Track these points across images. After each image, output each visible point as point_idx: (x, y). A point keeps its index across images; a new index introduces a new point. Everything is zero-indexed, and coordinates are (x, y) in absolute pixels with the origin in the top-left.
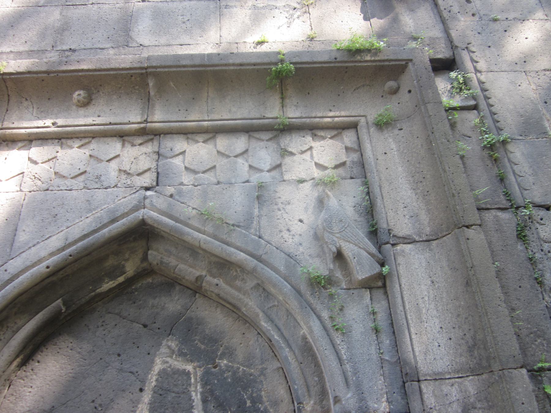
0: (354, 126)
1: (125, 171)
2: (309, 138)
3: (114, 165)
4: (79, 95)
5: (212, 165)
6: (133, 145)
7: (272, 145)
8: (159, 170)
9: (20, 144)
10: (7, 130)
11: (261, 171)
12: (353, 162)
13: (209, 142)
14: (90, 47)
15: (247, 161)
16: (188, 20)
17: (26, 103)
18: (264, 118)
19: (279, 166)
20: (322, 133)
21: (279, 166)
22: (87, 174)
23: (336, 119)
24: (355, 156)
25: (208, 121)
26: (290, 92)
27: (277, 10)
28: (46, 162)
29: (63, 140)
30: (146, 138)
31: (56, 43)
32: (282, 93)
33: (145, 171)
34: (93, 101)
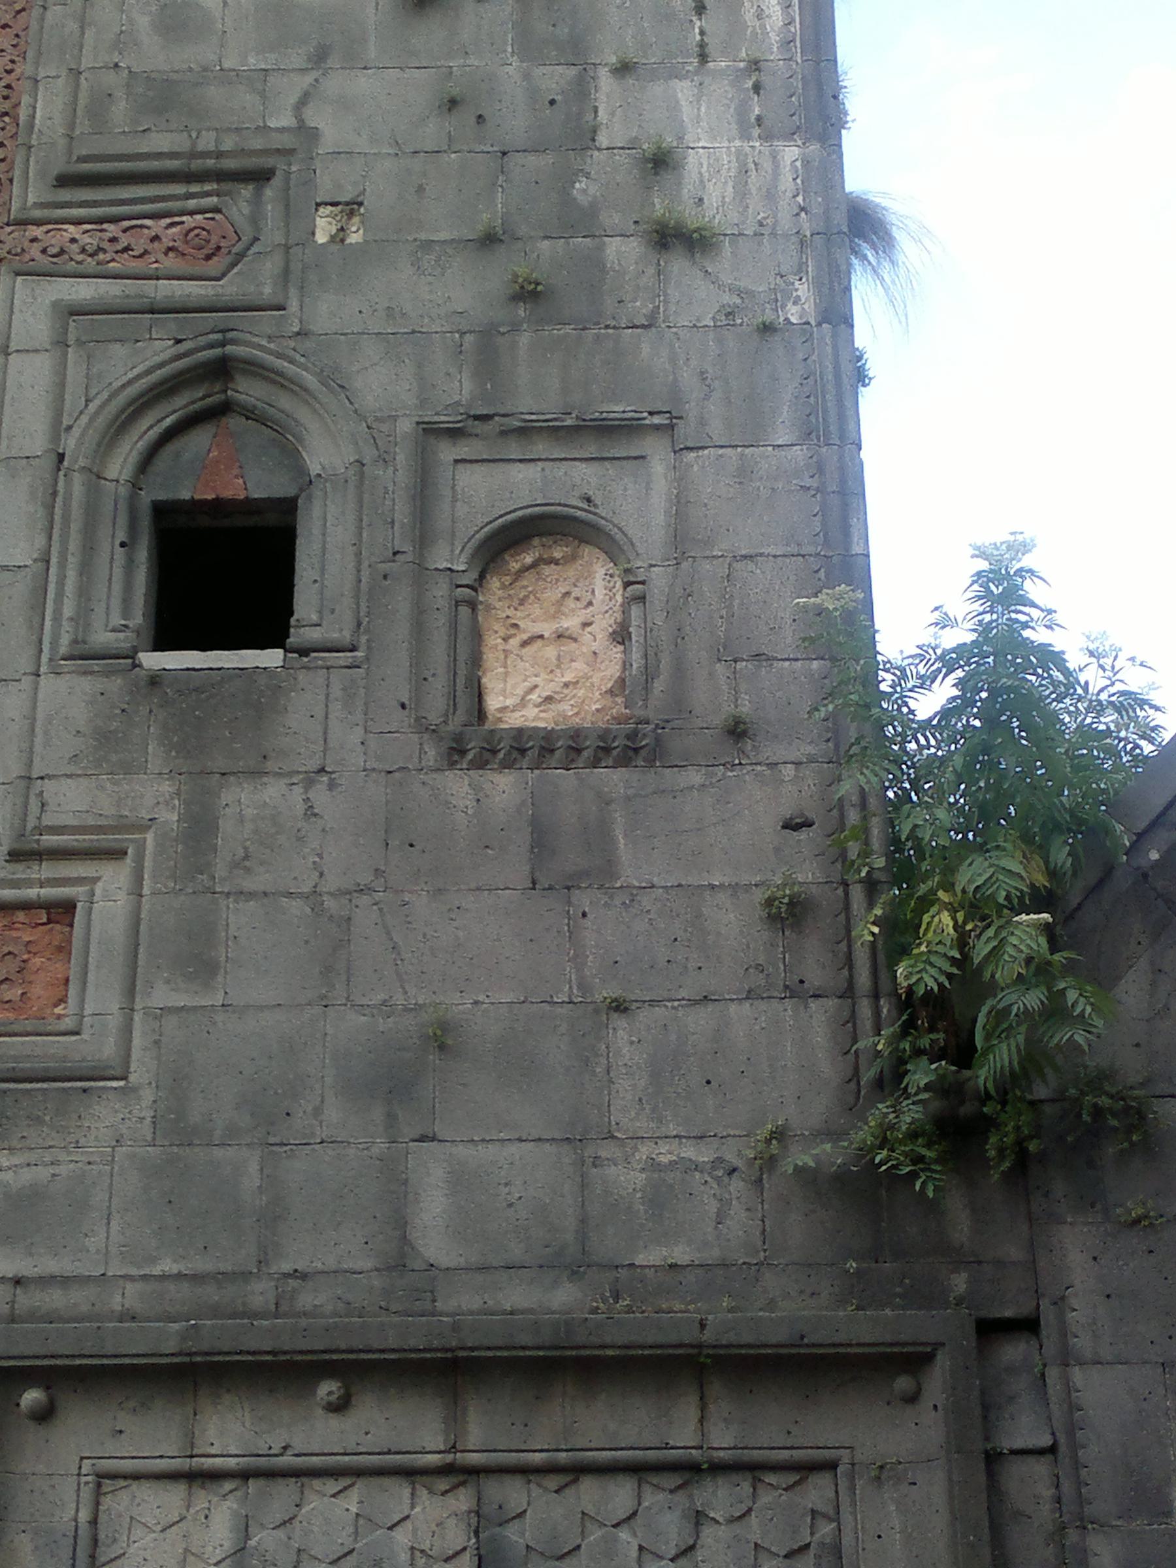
0: (831, 1466)
1: (422, 1551)
2: (746, 1487)
3: (402, 1538)
4: (330, 1393)
5: (575, 1545)
6: (431, 1492)
7: (681, 1498)
8: (482, 1552)
9: (228, 1486)
10: (203, 1460)
11: (661, 1558)
12: (822, 1544)
13: (567, 1491)
14: (334, 1267)
15: (635, 1535)
16: (520, 1198)
17: (227, 1399)
18: (667, 1447)
19: (692, 1548)
20: (771, 1478)
21: (692, 1548)
22: (355, 1554)
23: (797, 1454)
24: (826, 1529)
25: (566, 1451)
26: (715, 1388)
27: (697, 1175)
28: (279, 1526)
29: (305, 1480)
30: (454, 1480)
31: (266, 1254)
32: (702, 1387)
33: (457, 1554)
34: (353, 1399)
